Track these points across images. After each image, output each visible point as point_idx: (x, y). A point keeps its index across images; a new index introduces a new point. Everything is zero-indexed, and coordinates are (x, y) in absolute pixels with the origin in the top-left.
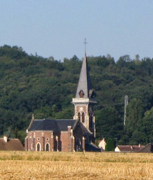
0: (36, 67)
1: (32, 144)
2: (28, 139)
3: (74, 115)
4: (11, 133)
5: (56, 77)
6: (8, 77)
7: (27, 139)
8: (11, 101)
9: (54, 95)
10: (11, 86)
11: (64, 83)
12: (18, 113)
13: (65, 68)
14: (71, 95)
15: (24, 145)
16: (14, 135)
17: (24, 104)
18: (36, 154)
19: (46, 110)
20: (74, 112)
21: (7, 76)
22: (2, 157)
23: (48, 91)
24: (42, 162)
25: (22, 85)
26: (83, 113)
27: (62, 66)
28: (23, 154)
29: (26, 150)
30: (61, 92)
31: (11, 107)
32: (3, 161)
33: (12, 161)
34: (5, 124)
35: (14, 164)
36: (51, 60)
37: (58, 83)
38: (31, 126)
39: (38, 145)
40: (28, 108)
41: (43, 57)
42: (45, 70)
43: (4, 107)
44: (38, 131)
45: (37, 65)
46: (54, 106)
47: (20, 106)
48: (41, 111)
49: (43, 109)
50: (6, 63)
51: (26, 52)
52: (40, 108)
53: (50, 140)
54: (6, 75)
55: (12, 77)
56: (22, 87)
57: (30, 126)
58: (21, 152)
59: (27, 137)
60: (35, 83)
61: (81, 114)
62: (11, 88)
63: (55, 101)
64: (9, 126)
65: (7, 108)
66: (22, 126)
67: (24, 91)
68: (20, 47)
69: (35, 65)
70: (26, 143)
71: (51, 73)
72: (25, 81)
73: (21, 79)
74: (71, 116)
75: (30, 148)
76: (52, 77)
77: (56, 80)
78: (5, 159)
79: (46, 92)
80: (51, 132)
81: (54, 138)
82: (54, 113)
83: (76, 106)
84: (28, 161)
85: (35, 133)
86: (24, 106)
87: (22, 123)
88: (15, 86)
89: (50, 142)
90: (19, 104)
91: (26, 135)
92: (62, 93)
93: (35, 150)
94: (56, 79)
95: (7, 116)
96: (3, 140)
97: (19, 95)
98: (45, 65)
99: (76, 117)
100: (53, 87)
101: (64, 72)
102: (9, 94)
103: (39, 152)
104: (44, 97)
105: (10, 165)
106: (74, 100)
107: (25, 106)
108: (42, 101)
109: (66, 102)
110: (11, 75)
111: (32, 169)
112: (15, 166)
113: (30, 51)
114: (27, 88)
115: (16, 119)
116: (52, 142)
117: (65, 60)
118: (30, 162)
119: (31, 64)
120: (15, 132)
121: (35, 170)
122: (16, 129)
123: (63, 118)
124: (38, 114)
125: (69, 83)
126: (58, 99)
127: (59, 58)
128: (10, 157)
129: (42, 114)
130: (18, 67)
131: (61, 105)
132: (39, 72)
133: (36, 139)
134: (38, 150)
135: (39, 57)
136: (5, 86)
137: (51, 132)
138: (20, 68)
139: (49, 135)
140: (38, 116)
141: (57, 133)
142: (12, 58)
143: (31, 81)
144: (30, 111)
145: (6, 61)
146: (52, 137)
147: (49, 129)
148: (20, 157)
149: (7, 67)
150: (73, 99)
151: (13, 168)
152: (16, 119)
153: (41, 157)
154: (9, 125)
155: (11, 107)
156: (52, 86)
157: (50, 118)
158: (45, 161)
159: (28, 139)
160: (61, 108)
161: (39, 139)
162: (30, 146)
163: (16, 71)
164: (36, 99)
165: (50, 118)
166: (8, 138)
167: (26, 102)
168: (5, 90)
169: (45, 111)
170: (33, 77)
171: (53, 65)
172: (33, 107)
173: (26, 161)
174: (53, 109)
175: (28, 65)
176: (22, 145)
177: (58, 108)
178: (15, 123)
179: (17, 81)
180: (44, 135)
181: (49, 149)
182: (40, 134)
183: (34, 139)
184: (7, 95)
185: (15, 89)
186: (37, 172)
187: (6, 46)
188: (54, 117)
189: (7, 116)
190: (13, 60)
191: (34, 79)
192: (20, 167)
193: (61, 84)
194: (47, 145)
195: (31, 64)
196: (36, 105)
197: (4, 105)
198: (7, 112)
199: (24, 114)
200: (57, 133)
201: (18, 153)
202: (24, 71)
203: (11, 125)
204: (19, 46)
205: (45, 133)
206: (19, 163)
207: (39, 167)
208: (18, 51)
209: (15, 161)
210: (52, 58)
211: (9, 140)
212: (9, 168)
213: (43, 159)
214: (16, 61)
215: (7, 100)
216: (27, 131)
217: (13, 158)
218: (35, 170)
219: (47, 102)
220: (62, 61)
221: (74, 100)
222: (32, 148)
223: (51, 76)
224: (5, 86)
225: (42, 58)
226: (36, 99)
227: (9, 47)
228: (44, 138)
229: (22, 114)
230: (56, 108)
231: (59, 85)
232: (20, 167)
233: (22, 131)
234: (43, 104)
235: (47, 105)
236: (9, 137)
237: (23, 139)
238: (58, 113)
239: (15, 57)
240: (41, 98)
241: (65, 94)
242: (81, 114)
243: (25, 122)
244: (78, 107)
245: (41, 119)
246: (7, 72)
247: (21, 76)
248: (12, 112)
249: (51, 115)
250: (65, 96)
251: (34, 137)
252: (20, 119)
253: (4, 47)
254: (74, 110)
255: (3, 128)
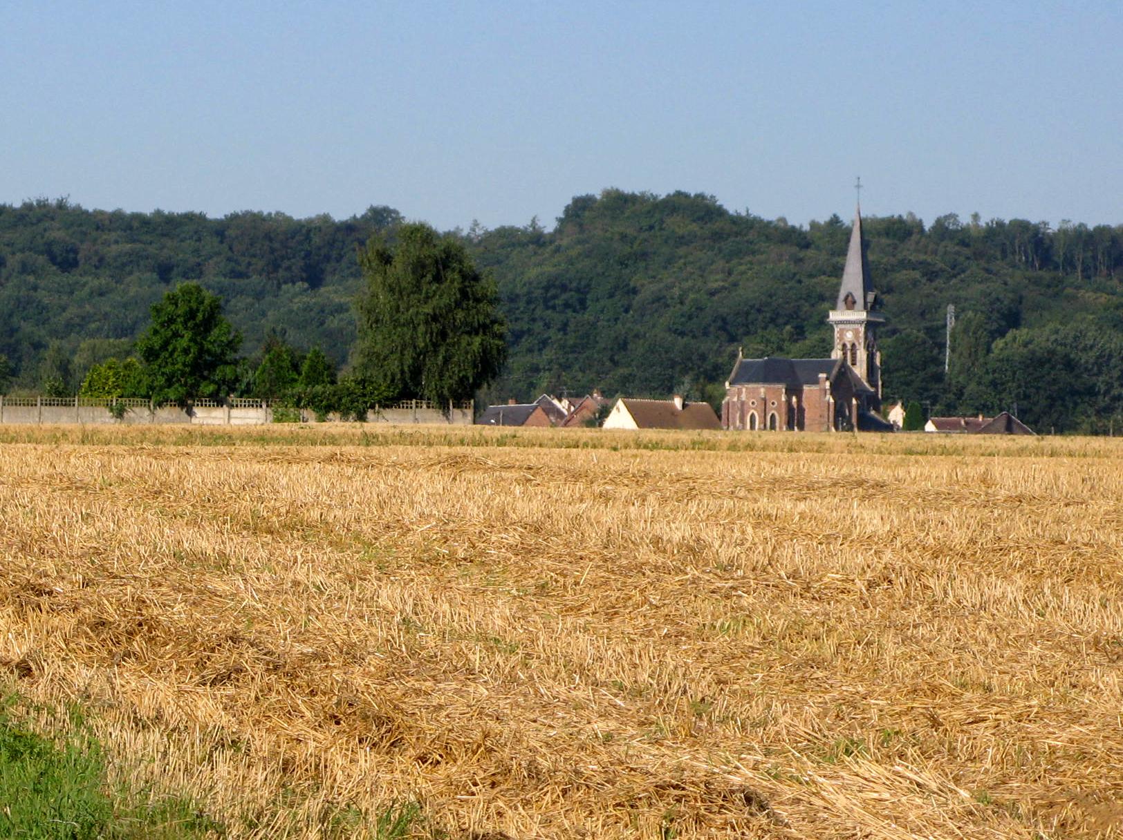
0: (747, 242)
1: (738, 415)
2: (728, 403)
3: (832, 348)
4: (691, 389)
5: (792, 263)
6: (685, 264)
7: (728, 403)
8: (690, 318)
9: (787, 303)
10: (690, 283)
11: (811, 276)
12: (706, 345)
13: (813, 242)
14: (826, 305)
15: (720, 417)
16: (698, 394)
17: (719, 323)
18: (746, 436)
19: (769, 337)
20: (833, 342)
21: (682, 261)
22: (671, 442)
23: (775, 295)
24: (761, 454)
25: (716, 281)
26: (853, 345)
27: (805, 238)
28: (721, 436)
29: (725, 427)
30: (804, 296)
31: (691, 331)
32: (673, 451)
33: (693, 452)
34: (678, 368)
35: (698, 459)
36: (782, 224)
37: (797, 277)
38: (737, 375)
39: (752, 416)
40: (729, 333)
41: (762, 217)
42: (768, 247)
43: (675, 331)
44: (751, 386)
45: (750, 237)
46: (788, 327)
47: (712, 329)
48: (759, 339)
49: (763, 337)
50: (680, 232)
51: (725, 207)
52: (756, 333)
53: (779, 404)
54: (680, 258)
55: (692, 263)
56: (715, 285)
57: (733, 374)
58: (713, 432)
59: (727, 399)
60: (744, 276)
61: (849, 346)
62: (691, 289)
63: (790, 318)
64: (687, 373)
65: (682, 334)
66: (716, 374)
67: (719, 295)
68: (712, 197)
69: (745, 235)
70: (724, 412)
71: (782, 255)
72: (723, 272)
73: (713, 267)
74: (827, 351)
75: (734, 423)
76: (784, 263)
77: (793, 271)
78: (676, 449)
79: (771, 296)
80: (782, 388)
81: (789, 402)
82: (787, 344)
83: (836, 330)
84: (729, 452)
85: (744, 390)
86: (720, 328)
87: (716, 367)
88: (699, 284)
89: (778, 409)
90: (710, 325)
91: (724, 395)
92: (806, 301)
93: (744, 427)
94: (793, 268)
95: (681, 352)
96: (673, 406)
97: (709, 304)
98: (767, 237)
99: (836, 354)
100: (786, 286)
101: (810, 253)
102: (687, 302)
103: (754, 432)
104: (766, 309)
105: (689, 462)
106: (834, 316)
107: (723, 329)
108: (760, 317)
109: (815, 320)
110: (691, 259)
111: (739, 472)
112: (700, 463)
113: (733, 204)
114: (726, 289)
115: (703, 357)
116: (784, 410)
117: (814, 225)
118: (734, 454)
119: (737, 234)
120: (700, 386)
121: (746, 473)
122: (701, 380)
123: (809, 355)
124: (751, 346)
125: (822, 277)
126: (795, 313)
127: (800, 219)
128: (688, 443)
129: (761, 347)
130: (707, 241)
131: (803, 327)
132: (753, 253)
133: (748, 403)
134: (752, 427)
135: (755, 218)
136: (677, 284)
137: (782, 388)
138: (712, 244)
139: (777, 394)
140: (751, 351)
141: (794, 390)
142: (694, 221)
143: (735, 273)
144: (733, 339)
145: (679, 226)
146: (783, 399)
147: (777, 380)
148: (710, 444)
149: (682, 241)
150: (831, 313)
151: (694, 469)
152: (703, 357)
153: (759, 443)
154: (685, 371)
155: (691, 331)
156: (784, 283)
157: (778, 356)
158: (767, 453)
159: (728, 403)
160: (804, 332)
161: (753, 403)
162: (734, 419)
163: (701, 250)
164: (747, 313)
165: (778, 356)
166: (684, 400)
167: (724, 320)
168: (676, 291)
169: (768, 341)
170: (741, 264)
171: (786, 236)
172: (741, 331)
173: (725, 454)
174: (785, 336)
175: (729, 235)
176: (717, 416)
177: (798, 334)
178: (699, 368)
179: (704, 271)
180: (765, 393)
181: (777, 424)
182: (755, 391)
183: (743, 403)
184: (682, 303)
185: (700, 291)
186: (749, 477)
187: (679, 194)
188: (788, 353)
189: (681, 352)
190: (694, 224)
191: (743, 268)
192: (712, 466)
193: (803, 279)
194: (773, 416)
195: (737, 234)
196: (747, 326)
197: (675, 327)
198: (682, 341)
199: (720, 347)
200: (794, 390)
201: (707, 434)
202: (720, 250)
203: (690, 372)
204: (708, 193)
205: (766, 388)
206: (709, 458)
207: (753, 465)
208: (707, 206)
209: (700, 452)
210: (783, 220)
211: (687, 405)
212: (686, 469)
213: (764, 449)
214: (702, 228)
215: (682, 315)
216: (727, 384)
217: (694, 445)
218: (746, 473)
219: (773, 320)
220: (806, 227)
221: (834, 316)
222: (738, 423)
223: (780, 261)
224: (677, 284)
225: (761, 221)
226: (747, 313)
227: (687, 196)
228: (765, 401)
229: (715, 348)
230: (792, 334)
231: (800, 282)
232: (712, 466)
233: (716, 385)
234: (763, 325)
235: (771, 326)
236: (685, 399)
237: (717, 402)
238: (798, 345)
239: (699, 219)
240: (759, 311)
241: (813, 301)
242: (849, 346)
243: (722, 364)
244: (842, 331)
245: (758, 357)
246: (682, 251)
247: (713, 262)
248: (692, 341)
249: (780, 349)
250: (813, 305)
251: (744, 399)
252: (712, 359)
253: (674, 195)
254: (832, 337)
255: (672, 377)
